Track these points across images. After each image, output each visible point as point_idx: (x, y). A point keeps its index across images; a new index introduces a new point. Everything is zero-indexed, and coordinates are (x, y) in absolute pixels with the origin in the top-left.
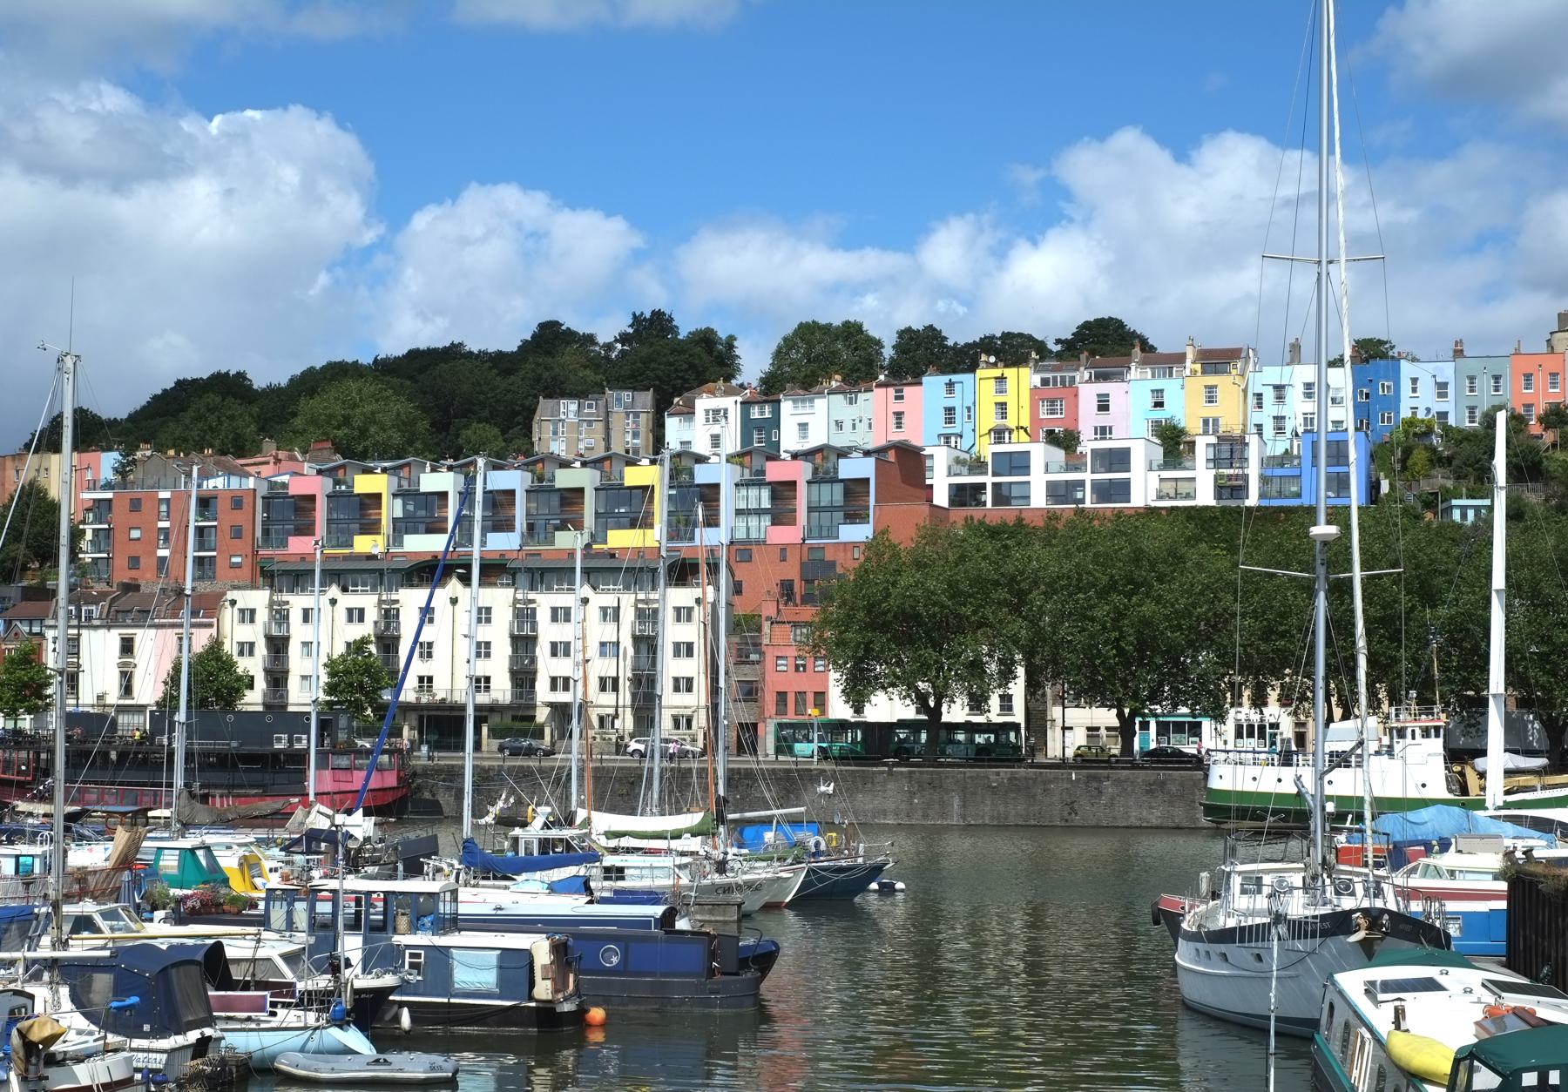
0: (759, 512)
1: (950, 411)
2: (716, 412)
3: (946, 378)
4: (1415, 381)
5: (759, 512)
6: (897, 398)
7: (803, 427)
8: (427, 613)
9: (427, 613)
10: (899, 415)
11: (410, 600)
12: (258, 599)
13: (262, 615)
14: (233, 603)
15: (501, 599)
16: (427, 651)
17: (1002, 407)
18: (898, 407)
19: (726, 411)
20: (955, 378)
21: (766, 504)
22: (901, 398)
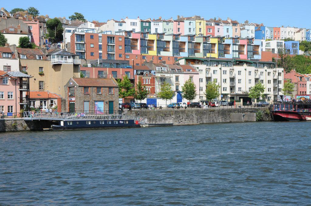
0: (236, 51)
1: (190, 29)
2: (134, 23)
3: (189, 21)
4: (267, 31)
5: (236, 51)
6: (178, 25)
7: (156, 29)
8: (239, 73)
9: (239, 73)
10: (179, 29)
11: (237, 68)
12: (203, 67)
13: (204, 71)
14: (198, 68)
15: (252, 69)
16: (239, 81)
17: (200, 29)
18: (178, 27)
19: (136, 23)
20: (191, 21)
21: (237, 49)
22: (179, 25)
